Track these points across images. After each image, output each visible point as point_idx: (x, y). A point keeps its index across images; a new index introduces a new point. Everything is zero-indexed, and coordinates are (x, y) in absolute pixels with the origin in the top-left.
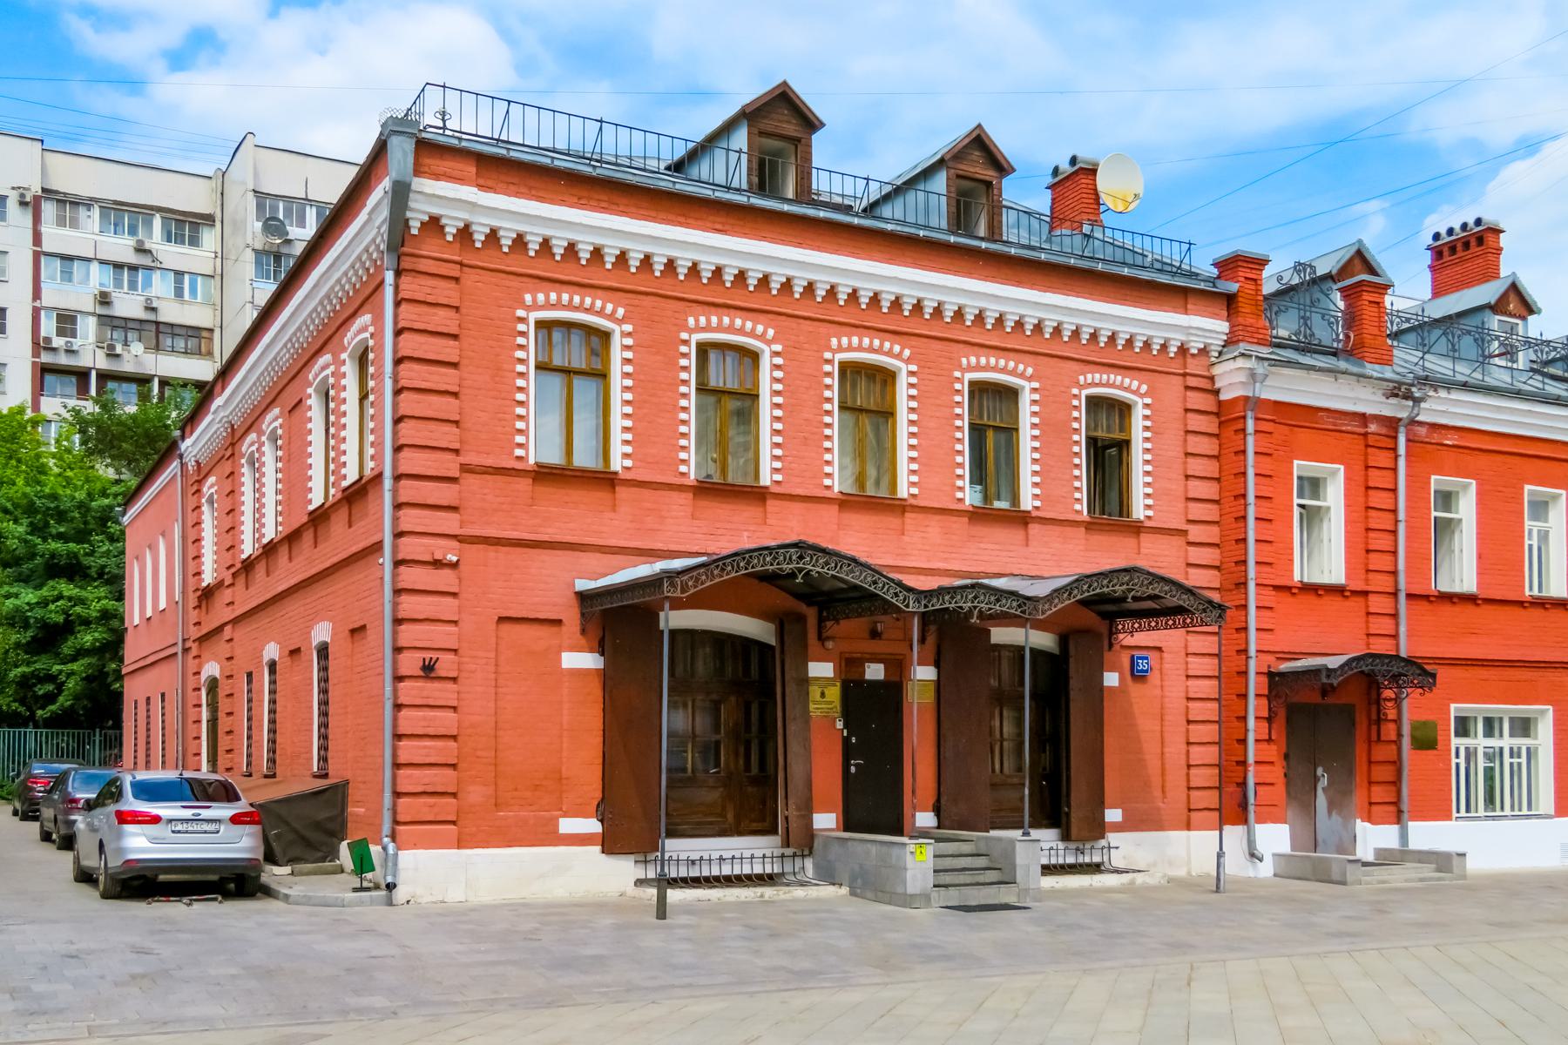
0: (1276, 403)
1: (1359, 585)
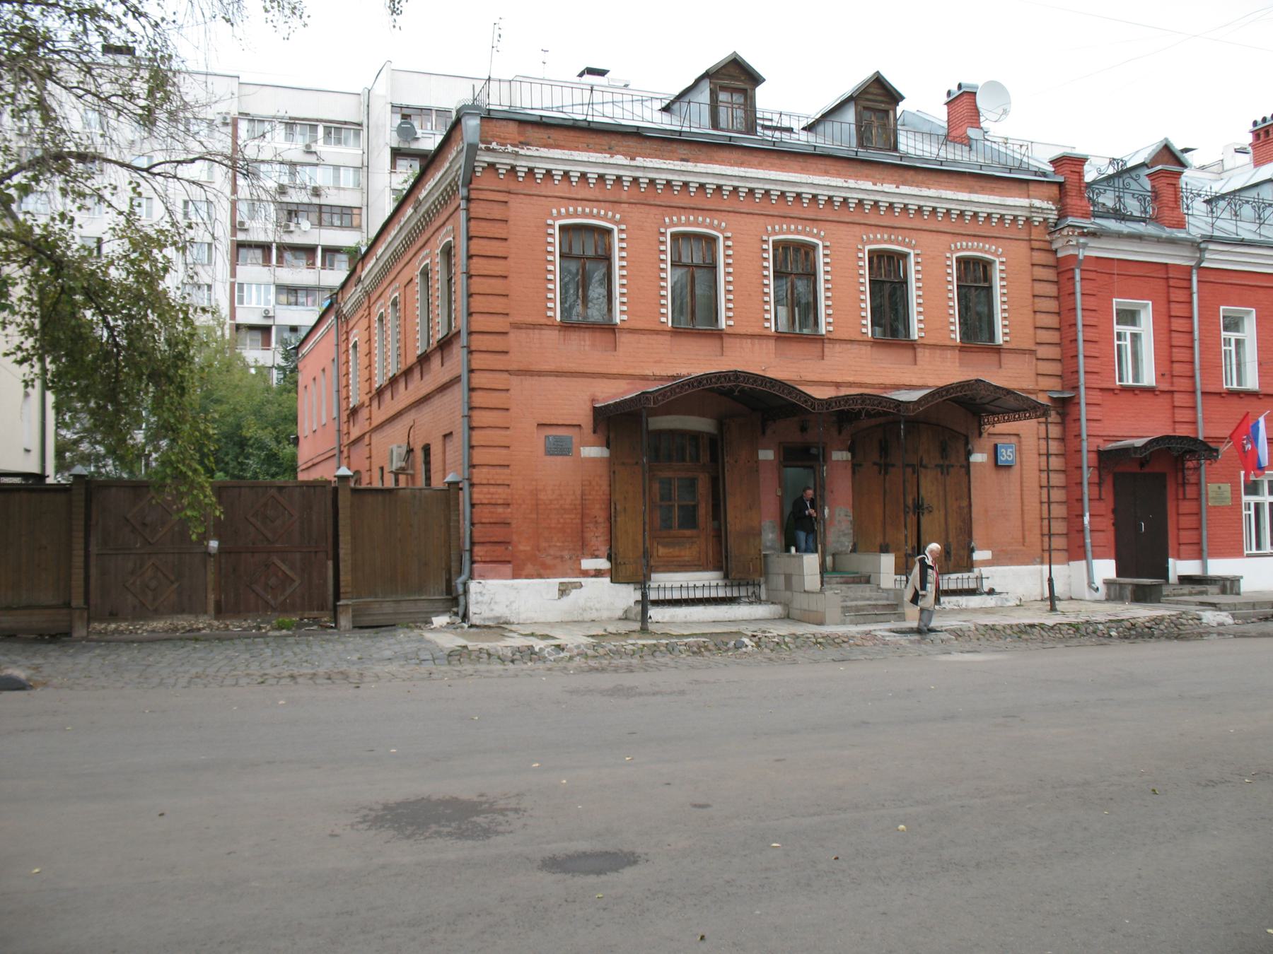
1: (1165, 386)
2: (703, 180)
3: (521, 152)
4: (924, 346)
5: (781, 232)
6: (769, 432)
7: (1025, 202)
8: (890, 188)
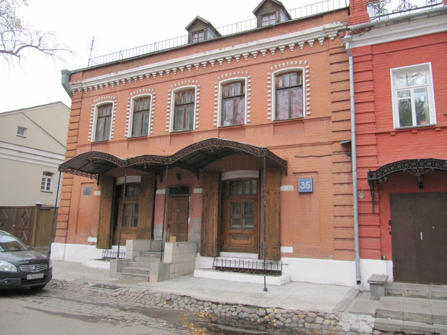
0: (372, 46)
2: (143, 73)
3: (83, 82)
4: (250, 127)
5: (178, 86)
6: (164, 181)
7: (320, 28)
8: (230, 48)
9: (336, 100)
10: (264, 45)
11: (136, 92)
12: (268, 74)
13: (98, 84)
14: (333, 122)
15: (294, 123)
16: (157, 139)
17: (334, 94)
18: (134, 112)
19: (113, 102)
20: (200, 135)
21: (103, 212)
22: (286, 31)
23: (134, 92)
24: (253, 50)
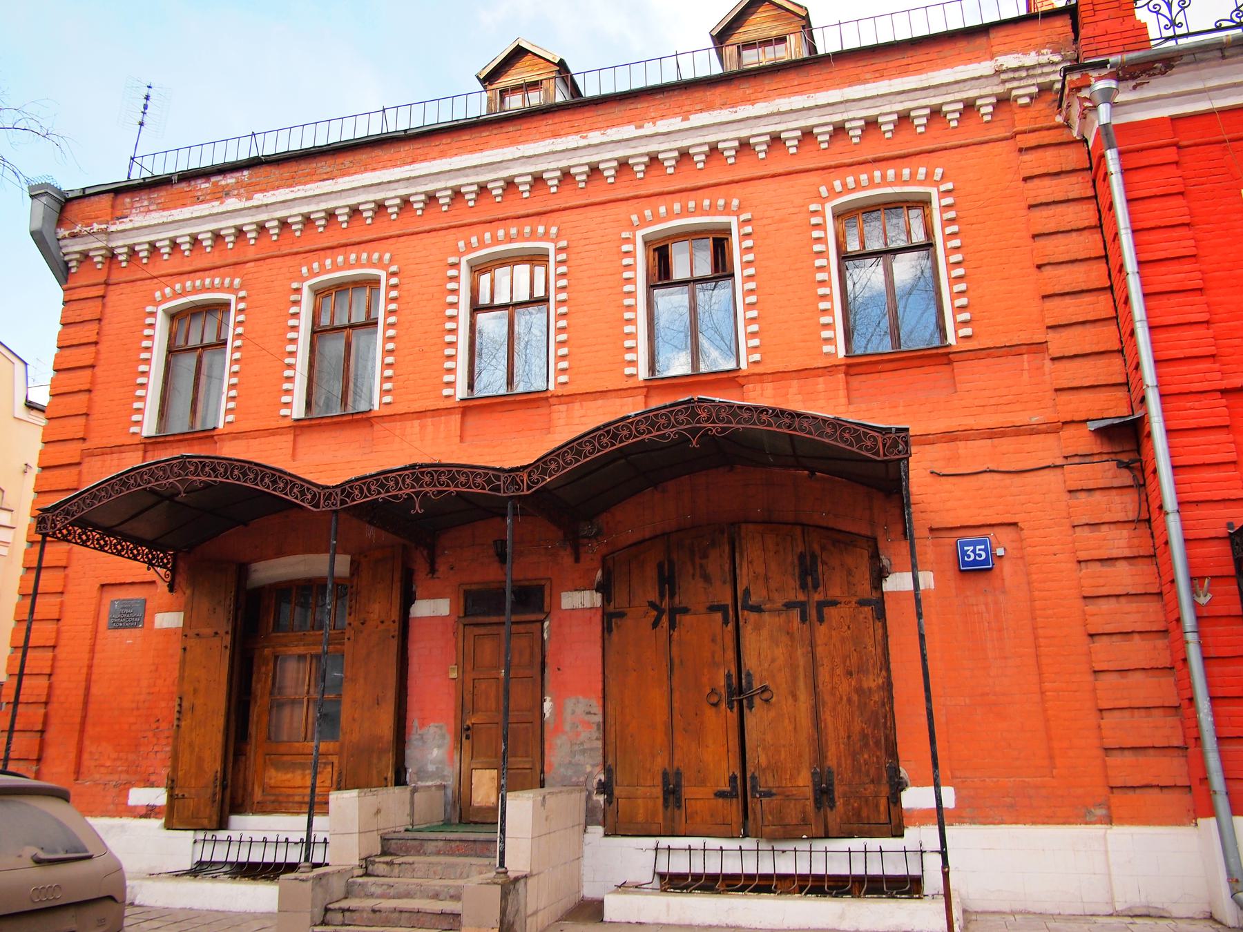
0: (1174, 119)
2: (353, 201)
3: (113, 228)
6: (442, 568)
7: (986, 67)
8: (675, 123)
9: (1057, 290)
10: (794, 116)
11: (322, 266)
12: (813, 207)
13: (171, 234)
14: (1053, 359)
15: (916, 362)
16: (408, 423)
17: (1048, 271)
18: (313, 332)
19: (233, 298)
20: (577, 405)
21: (195, 691)
22: (868, 76)
23: (316, 265)
24: (756, 131)
